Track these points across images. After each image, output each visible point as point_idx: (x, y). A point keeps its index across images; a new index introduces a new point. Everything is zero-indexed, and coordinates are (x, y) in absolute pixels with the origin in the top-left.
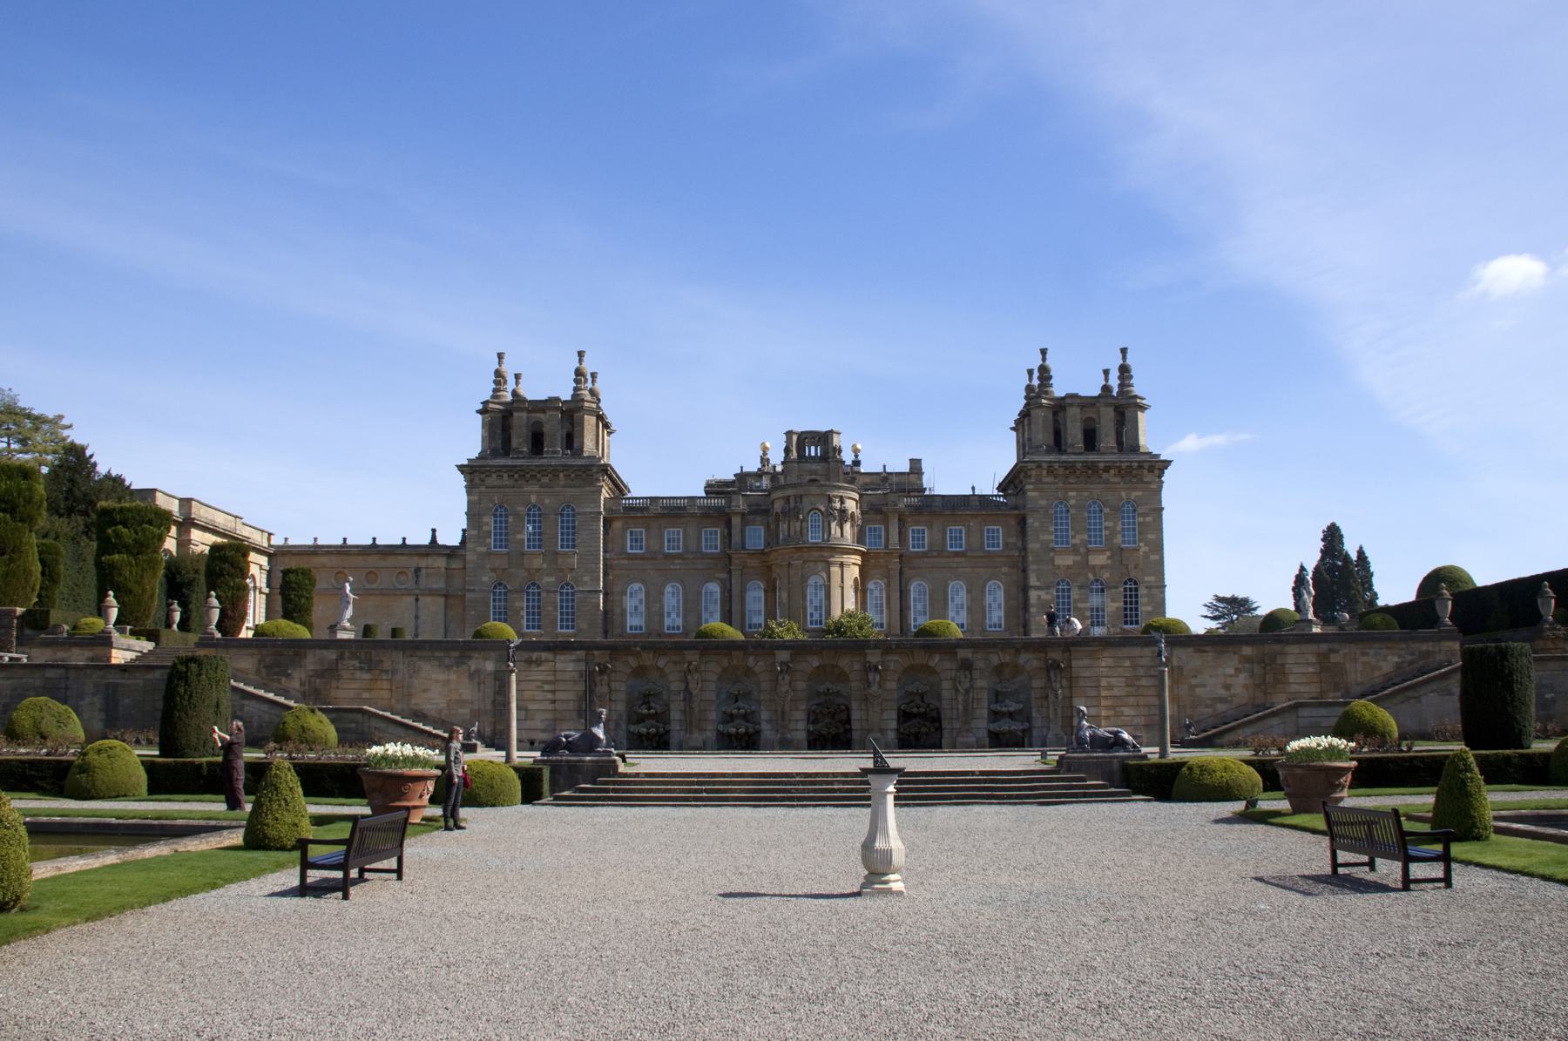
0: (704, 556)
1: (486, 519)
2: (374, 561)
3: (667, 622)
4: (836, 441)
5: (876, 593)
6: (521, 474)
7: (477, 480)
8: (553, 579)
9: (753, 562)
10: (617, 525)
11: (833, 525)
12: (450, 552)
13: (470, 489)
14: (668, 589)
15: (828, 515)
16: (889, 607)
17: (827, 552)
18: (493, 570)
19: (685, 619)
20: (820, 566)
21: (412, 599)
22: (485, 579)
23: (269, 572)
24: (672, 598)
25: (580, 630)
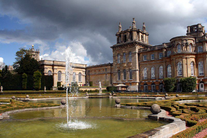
0: (159, 60)
1: (116, 57)
2: (100, 68)
3: (152, 76)
4: (200, 26)
5: (201, 65)
6: (121, 46)
7: (114, 49)
8: (128, 68)
9: (168, 60)
10: (141, 55)
11: (183, 48)
12: (111, 65)
13: (114, 51)
14: (152, 68)
15: (182, 45)
16: (204, 69)
17: (184, 55)
18: (118, 68)
19: (155, 75)
20: (180, 59)
21: (105, 75)
22: (116, 69)
23: (86, 72)
24: (153, 71)
25: (133, 79)
